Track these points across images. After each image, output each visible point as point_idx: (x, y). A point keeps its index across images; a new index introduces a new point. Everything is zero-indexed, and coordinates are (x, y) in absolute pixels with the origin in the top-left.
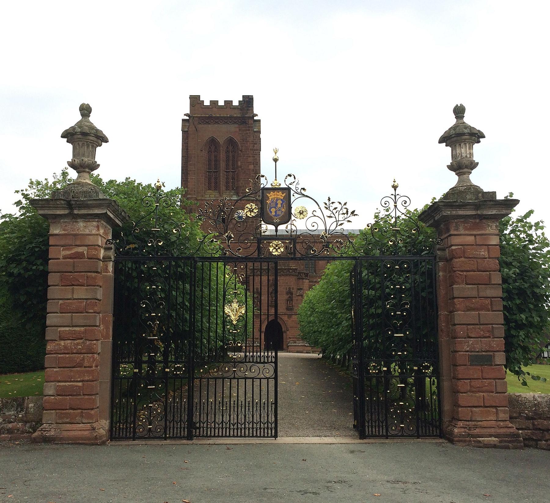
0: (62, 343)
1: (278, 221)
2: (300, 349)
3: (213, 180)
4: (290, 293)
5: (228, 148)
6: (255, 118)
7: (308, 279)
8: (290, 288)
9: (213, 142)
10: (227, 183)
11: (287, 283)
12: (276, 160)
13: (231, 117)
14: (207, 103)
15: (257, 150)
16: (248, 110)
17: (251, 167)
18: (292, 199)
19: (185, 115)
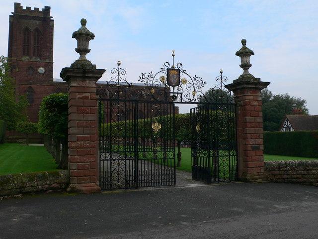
0: (79, 142)
1: (174, 84)
10: (34, 52)
12: (173, 56)
14: (24, 8)
18: (181, 75)
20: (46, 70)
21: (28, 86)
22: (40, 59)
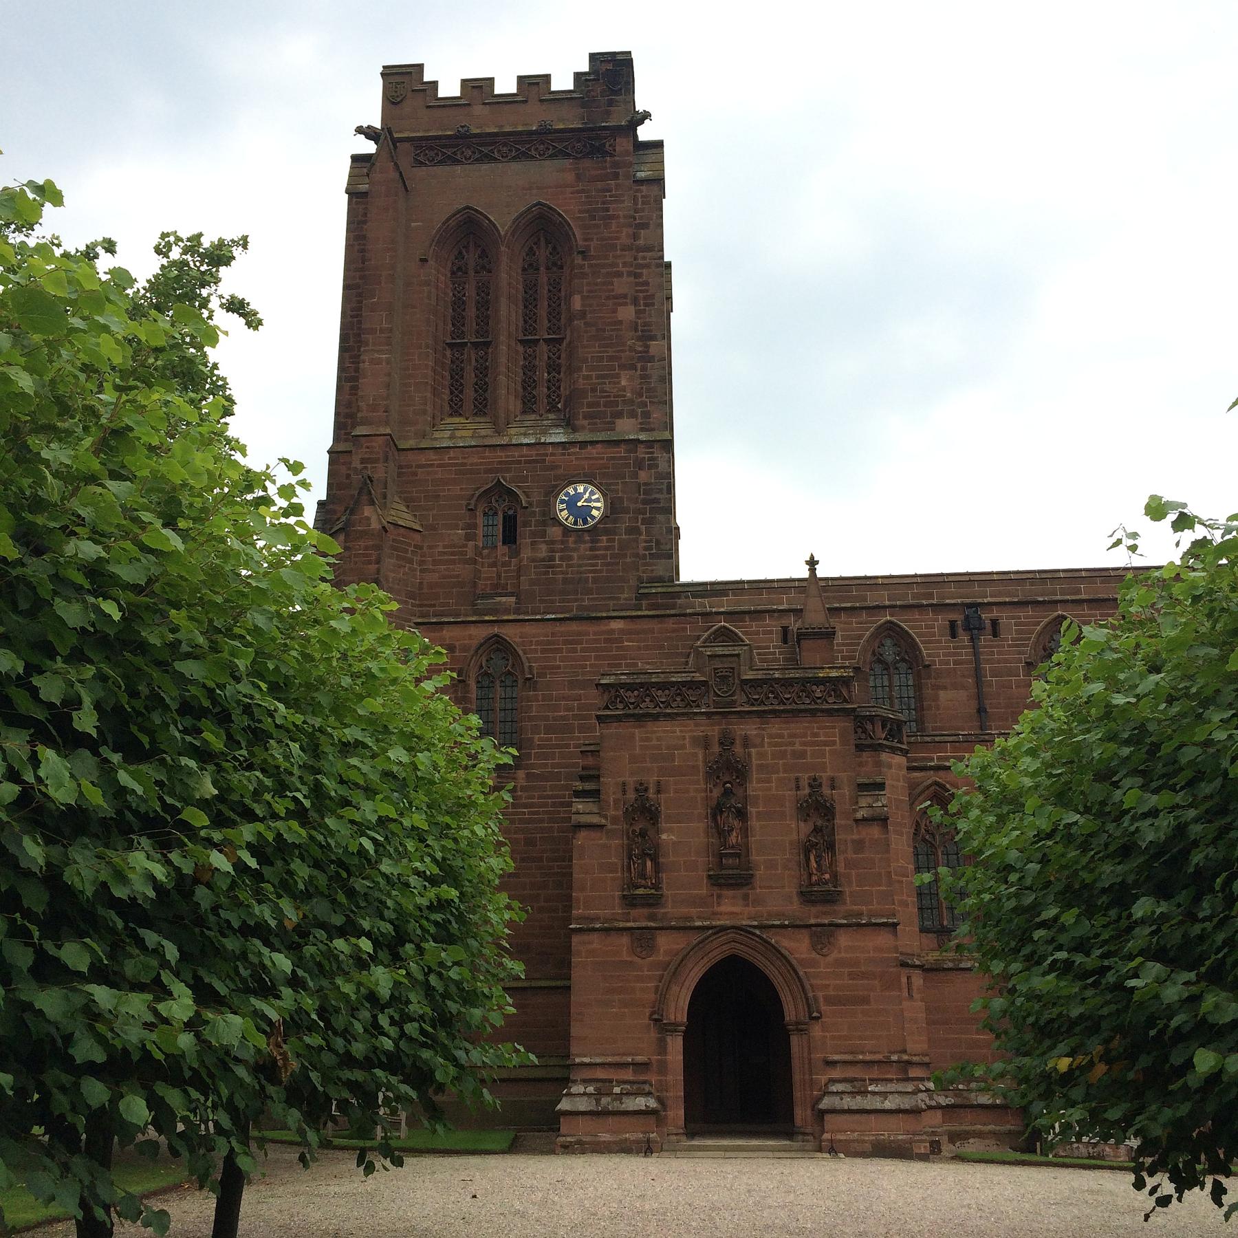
2: (895, 1131)
3: (470, 377)
4: (817, 808)
5: (531, 252)
6: (645, 133)
7: (905, 753)
8: (815, 784)
9: (469, 232)
10: (529, 384)
11: (802, 755)
13: (544, 133)
14: (449, 89)
15: (649, 249)
16: (611, 103)
17: (627, 313)
19: (360, 130)
20: (614, 508)
21: (481, 633)
22: (569, 424)
